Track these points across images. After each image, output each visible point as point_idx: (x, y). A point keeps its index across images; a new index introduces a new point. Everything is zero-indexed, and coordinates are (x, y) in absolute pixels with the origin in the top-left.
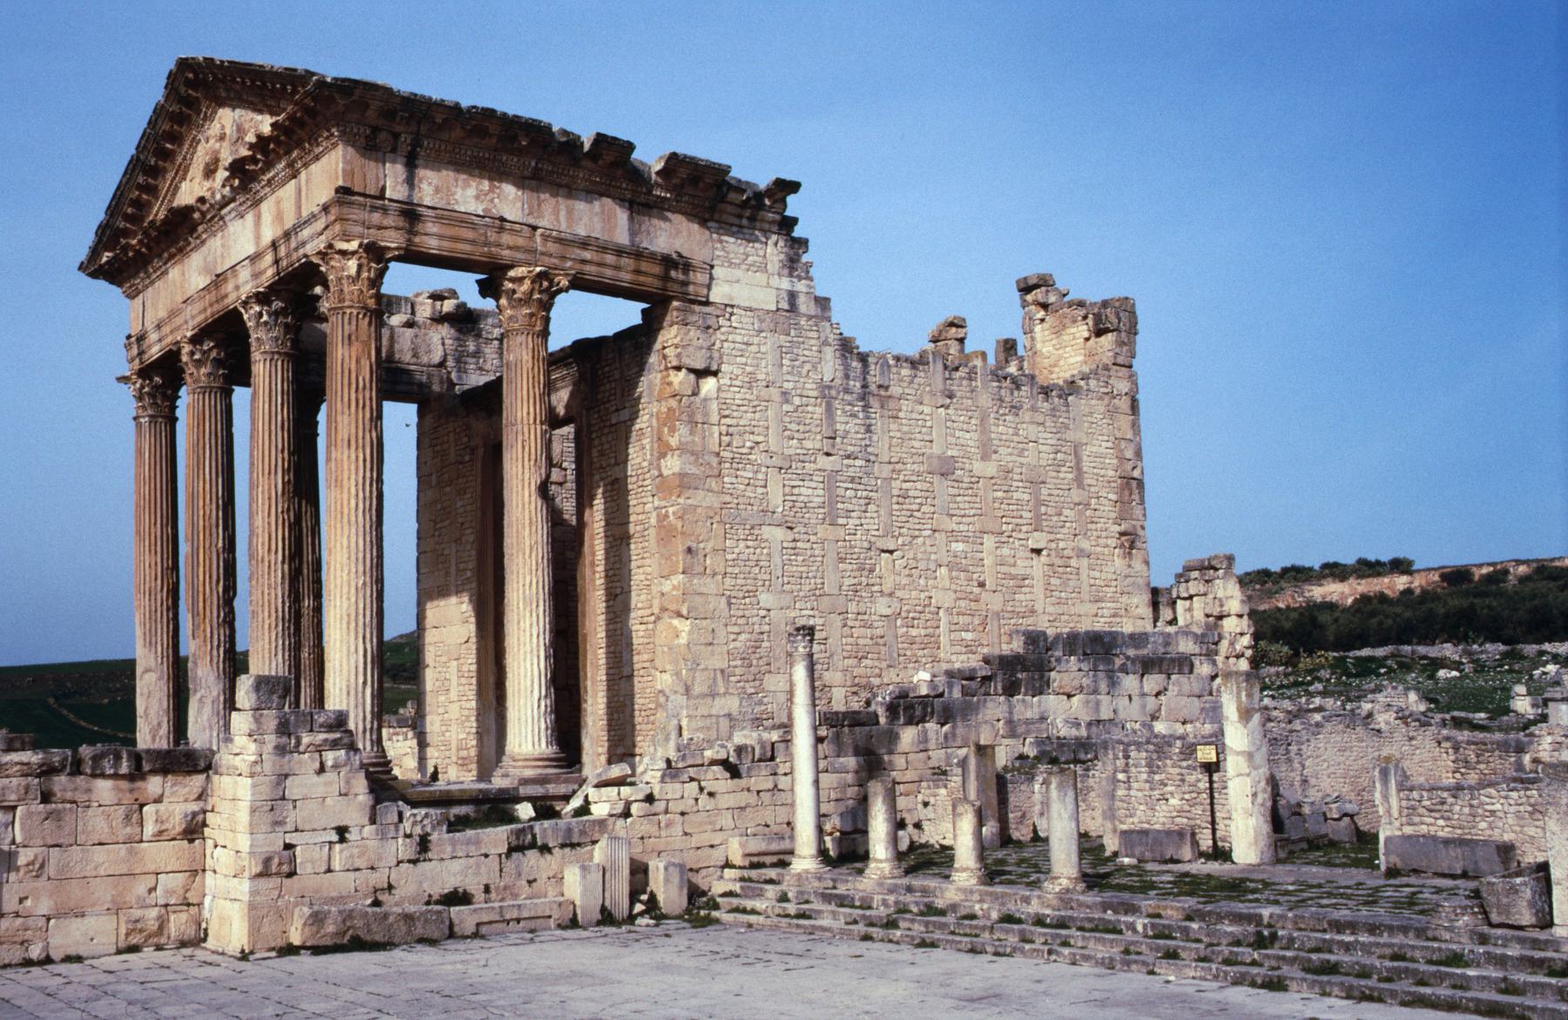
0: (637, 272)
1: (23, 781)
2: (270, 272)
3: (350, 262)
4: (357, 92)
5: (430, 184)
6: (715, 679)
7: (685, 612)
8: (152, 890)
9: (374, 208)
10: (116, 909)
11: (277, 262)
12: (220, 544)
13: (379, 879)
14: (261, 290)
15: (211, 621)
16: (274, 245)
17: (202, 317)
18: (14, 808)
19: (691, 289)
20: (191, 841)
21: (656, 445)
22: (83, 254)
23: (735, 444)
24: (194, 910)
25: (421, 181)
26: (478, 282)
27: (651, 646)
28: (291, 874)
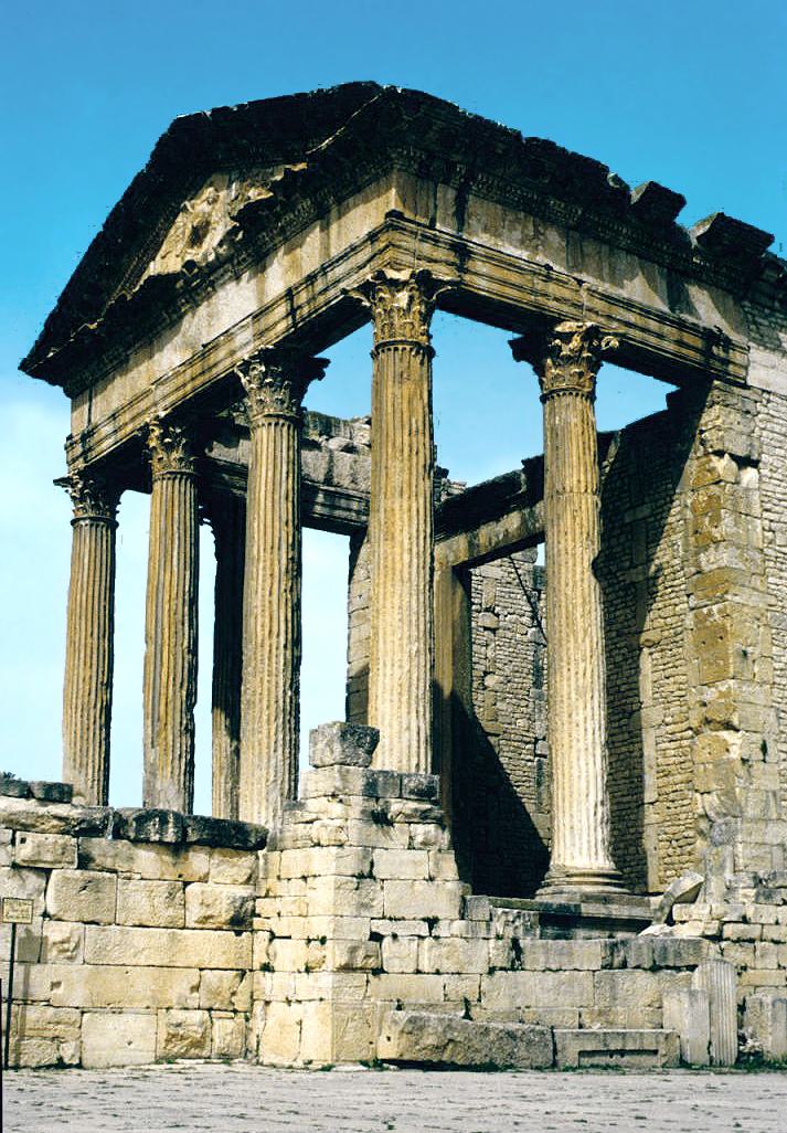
0: (680, 343)
1: (62, 839)
2: (282, 326)
3: (399, 295)
4: (423, 109)
5: (479, 220)
6: (767, 802)
7: (735, 722)
8: (196, 988)
9: (425, 238)
10: (160, 1007)
11: (292, 312)
12: (186, 644)
13: (466, 987)
14: (270, 347)
15: (173, 727)
16: (290, 294)
17: (181, 393)
18: (48, 872)
19: (731, 368)
20: (238, 933)
21: (692, 540)
22: (25, 349)
23: (778, 542)
24: (240, 1018)
25: (469, 218)
26: (512, 343)
27: (688, 764)
28: (378, 971)
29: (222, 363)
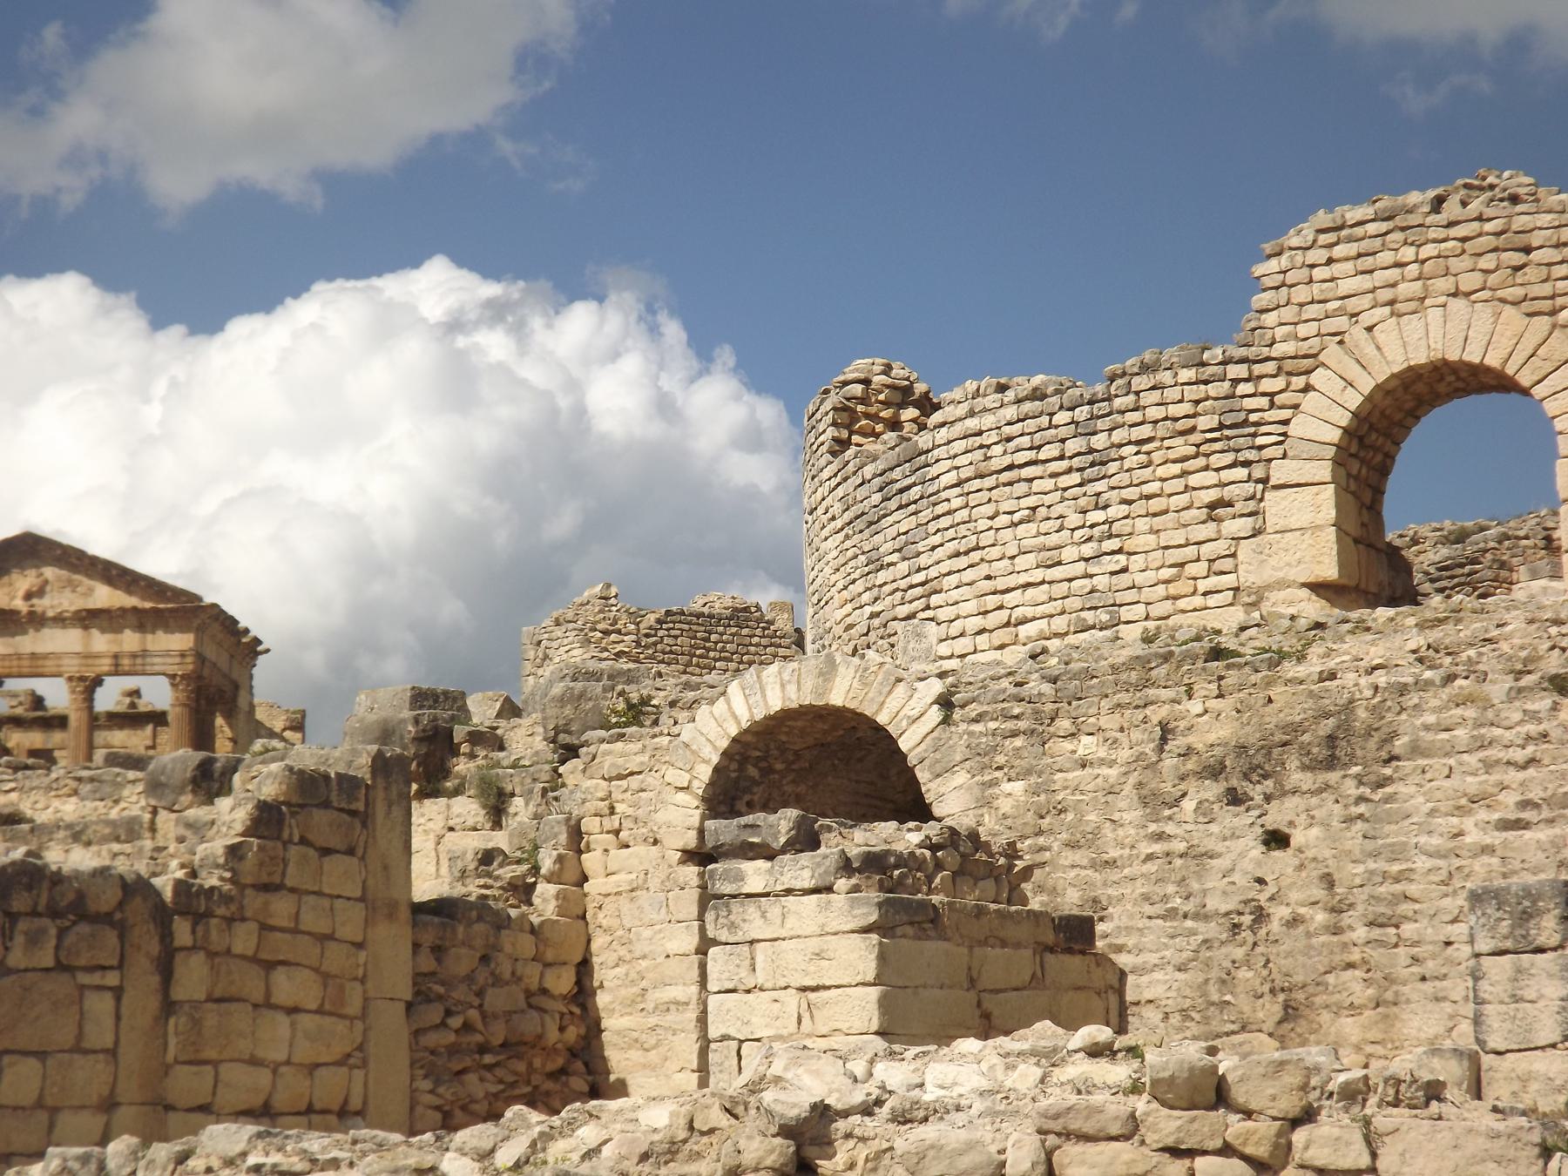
11: (117, 665)
16: (116, 656)
17: (7, 671)
29: (50, 665)
